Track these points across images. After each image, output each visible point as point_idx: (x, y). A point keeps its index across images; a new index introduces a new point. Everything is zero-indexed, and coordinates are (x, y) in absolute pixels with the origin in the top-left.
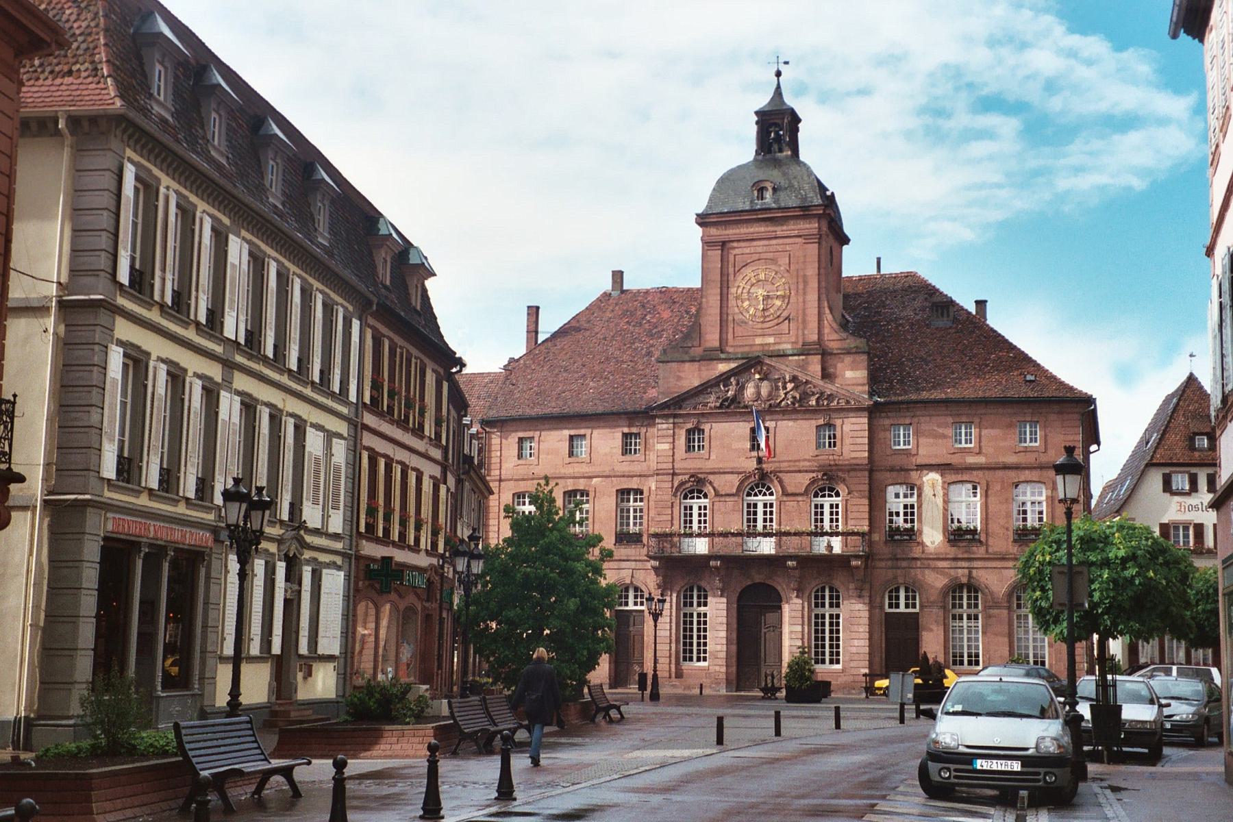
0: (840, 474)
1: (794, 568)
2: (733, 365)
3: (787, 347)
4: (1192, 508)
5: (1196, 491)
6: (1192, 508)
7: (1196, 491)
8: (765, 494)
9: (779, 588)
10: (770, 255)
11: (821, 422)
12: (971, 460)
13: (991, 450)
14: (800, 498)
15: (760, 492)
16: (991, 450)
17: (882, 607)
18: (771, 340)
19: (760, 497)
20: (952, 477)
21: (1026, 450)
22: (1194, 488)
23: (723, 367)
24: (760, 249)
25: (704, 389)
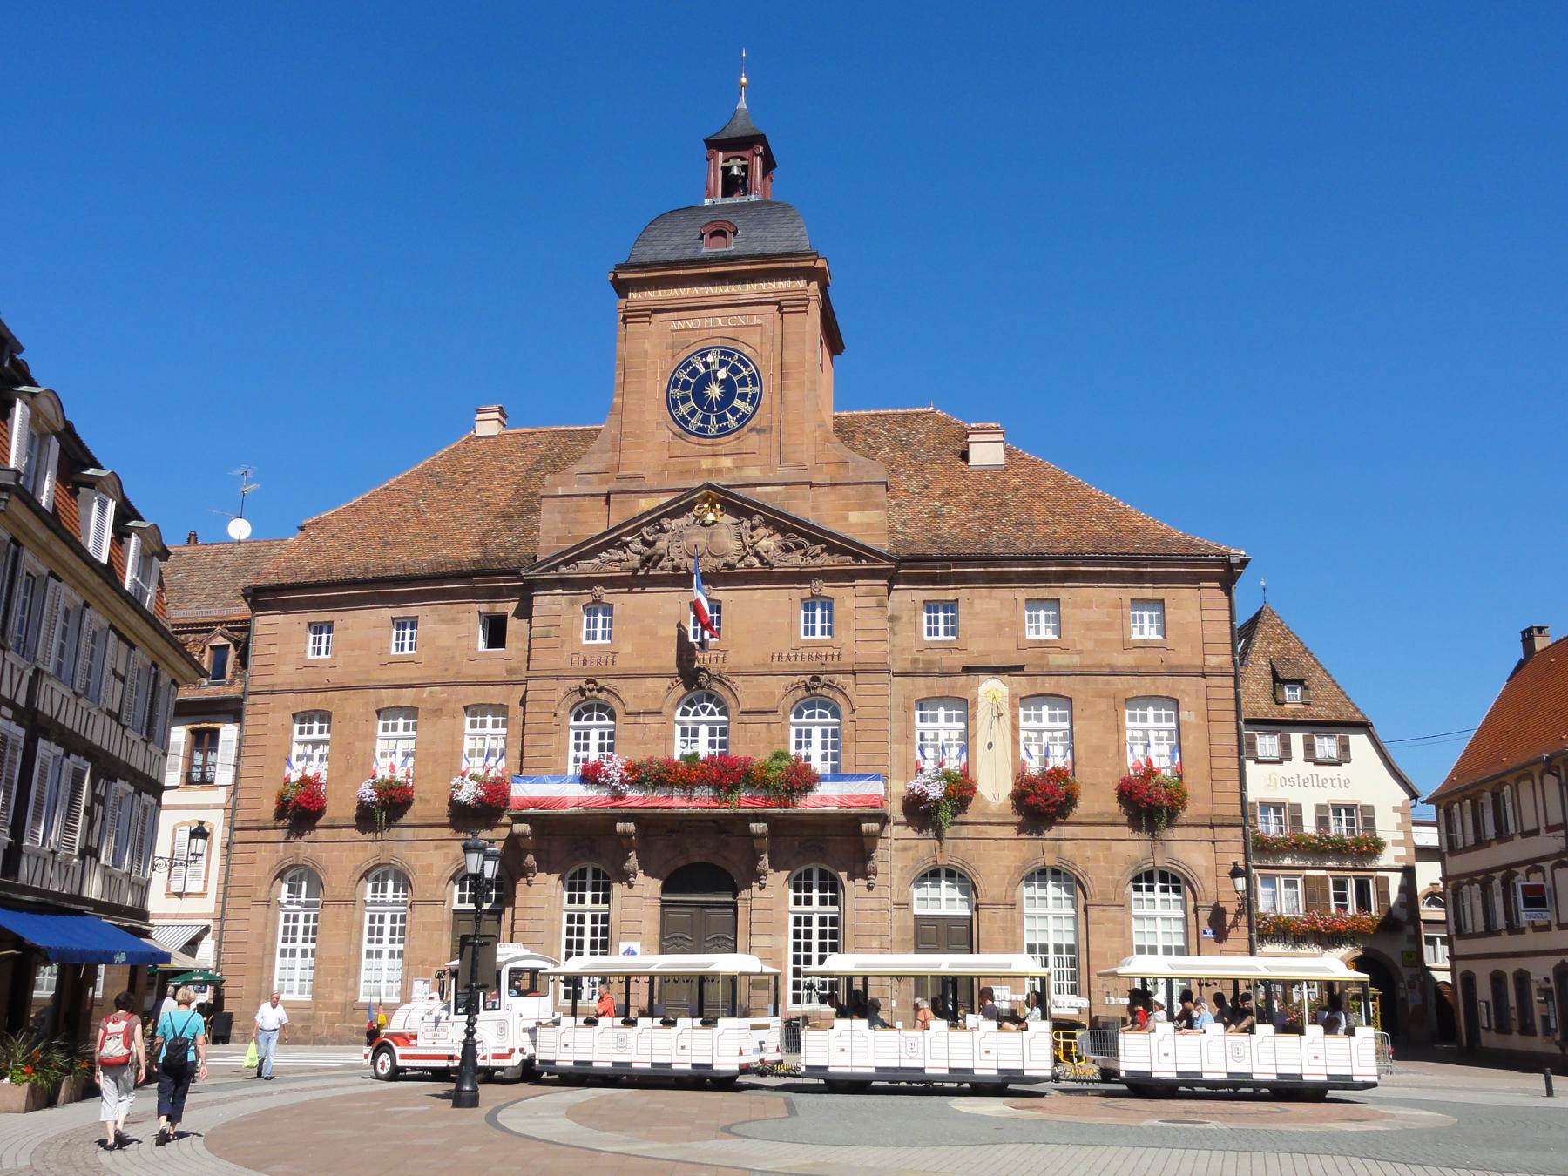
0: (840, 679)
1: (761, 836)
2: (664, 499)
3: (752, 473)
4: (1284, 782)
5: (1290, 759)
6: (1284, 782)
7: (1290, 759)
8: (712, 713)
9: (733, 872)
10: (730, 333)
11: (807, 593)
12: (1057, 660)
13: (1090, 645)
14: (771, 718)
15: (704, 709)
16: (1090, 645)
17: (906, 905)
18: (726, 462)
19: (704, 717)
20: (1021, 684)
21: (1145, 645)
22: (1286, 753)
23: (646, 504)
24: (712, 322)
25: (611, 541)
